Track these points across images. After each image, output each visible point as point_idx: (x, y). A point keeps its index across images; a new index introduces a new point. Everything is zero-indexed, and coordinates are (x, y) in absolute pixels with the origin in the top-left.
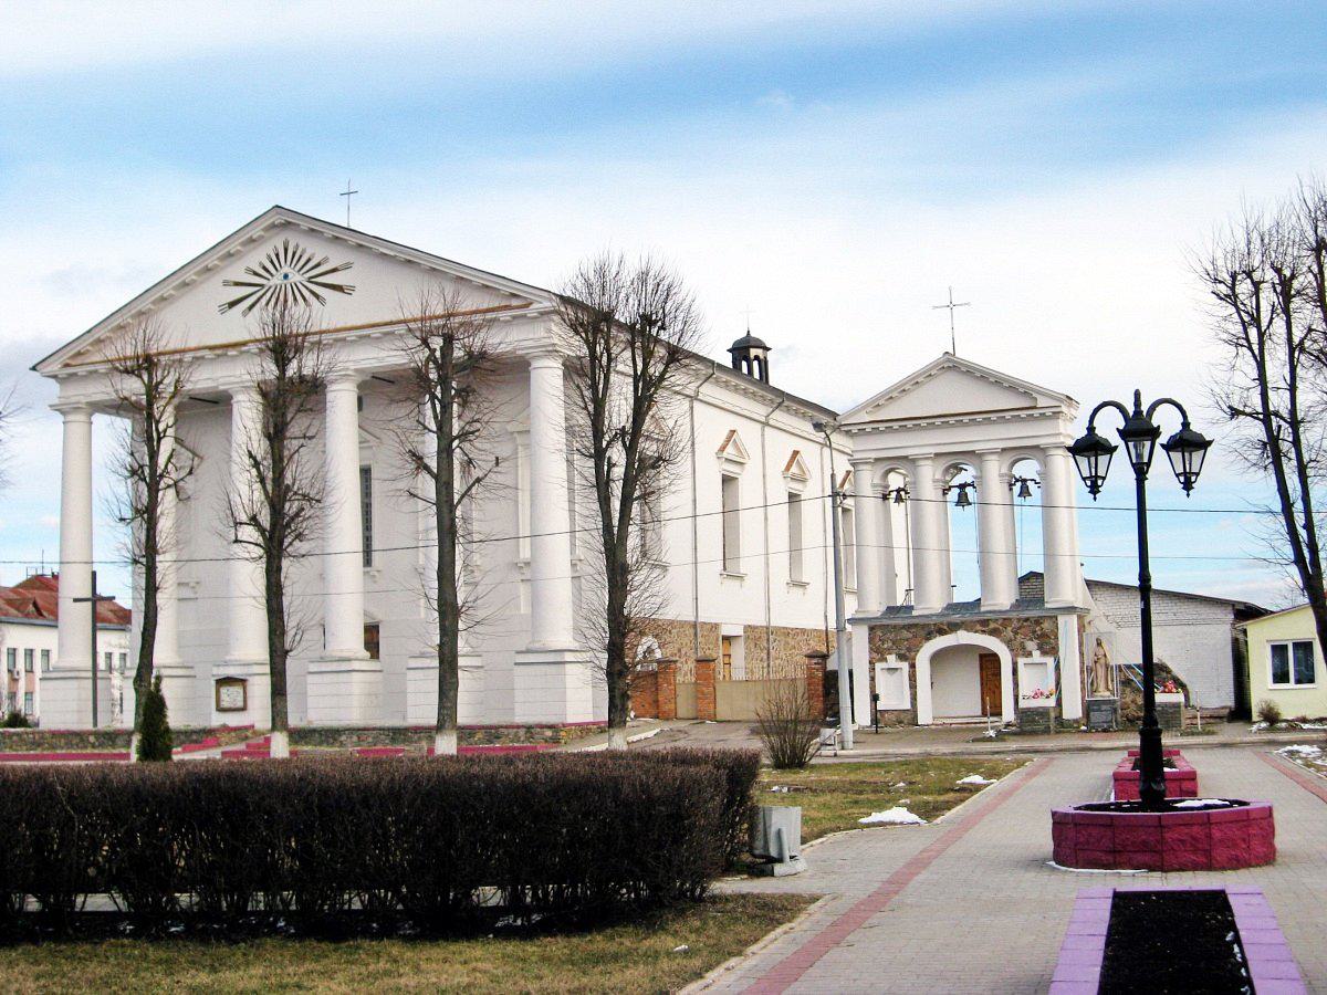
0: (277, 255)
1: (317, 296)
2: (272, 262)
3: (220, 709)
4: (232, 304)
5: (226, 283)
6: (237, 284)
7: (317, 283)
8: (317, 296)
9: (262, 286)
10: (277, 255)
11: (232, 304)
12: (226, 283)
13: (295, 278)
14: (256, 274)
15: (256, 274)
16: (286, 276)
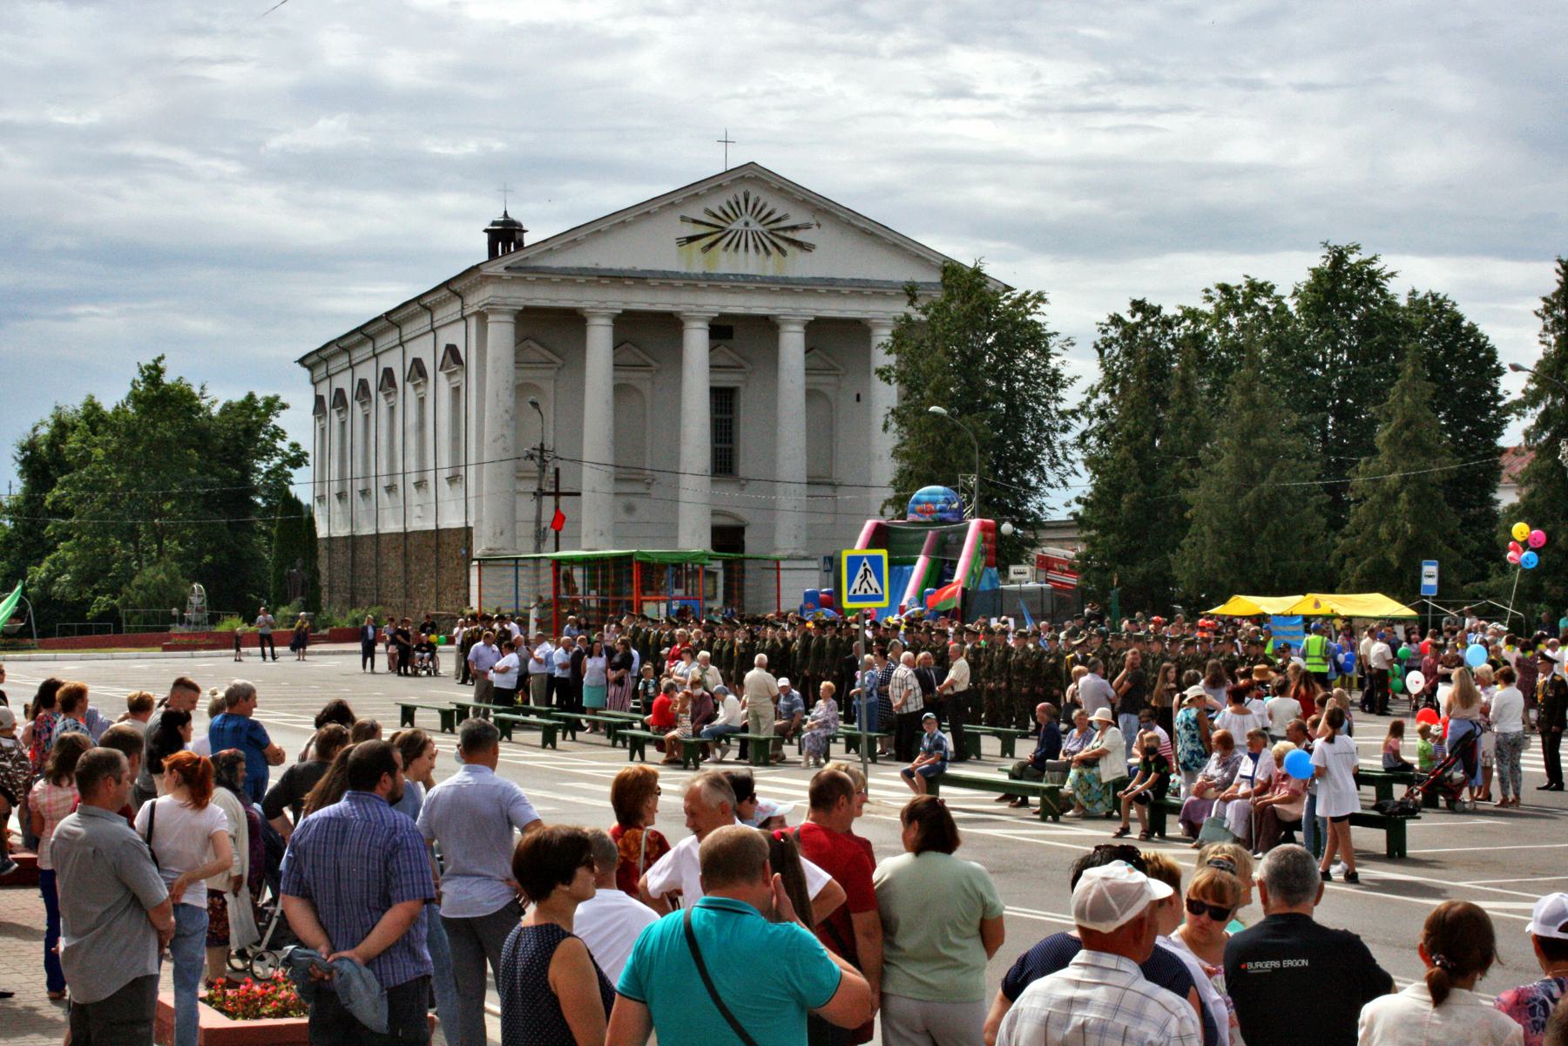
0: (738, 203)
1: (778, 248)
2: (732, 208)
3: (714, 597)
4: (691, 239)
5: (683, 219)
6: (695, 221)
7: (777, 236)
8: (778, 248)
9: (723, 229)
10: (738, 203)
11: (691, 239)
12: (683, 219)
13: (755, 226)
14: (715, 216)
15: (715, 216)
16: (747, 224)
